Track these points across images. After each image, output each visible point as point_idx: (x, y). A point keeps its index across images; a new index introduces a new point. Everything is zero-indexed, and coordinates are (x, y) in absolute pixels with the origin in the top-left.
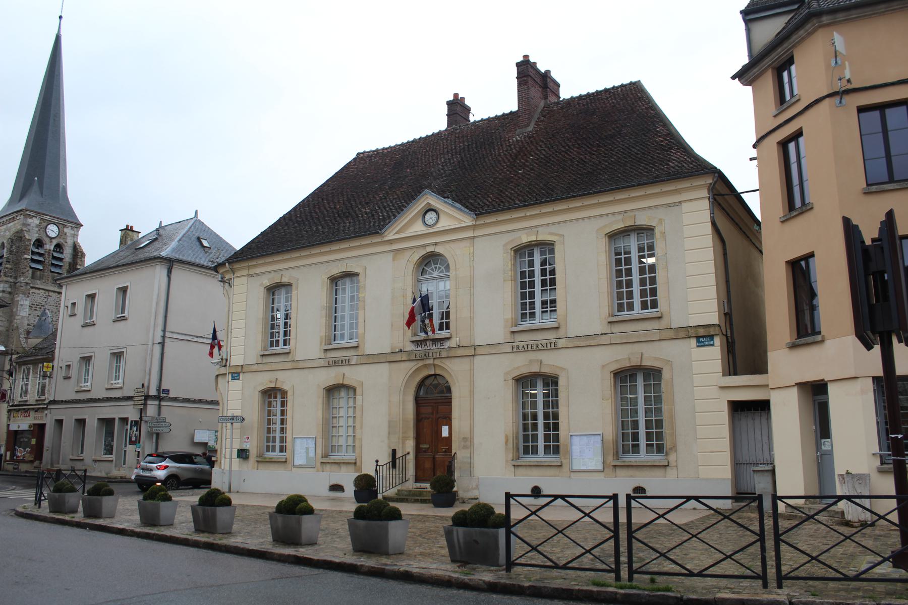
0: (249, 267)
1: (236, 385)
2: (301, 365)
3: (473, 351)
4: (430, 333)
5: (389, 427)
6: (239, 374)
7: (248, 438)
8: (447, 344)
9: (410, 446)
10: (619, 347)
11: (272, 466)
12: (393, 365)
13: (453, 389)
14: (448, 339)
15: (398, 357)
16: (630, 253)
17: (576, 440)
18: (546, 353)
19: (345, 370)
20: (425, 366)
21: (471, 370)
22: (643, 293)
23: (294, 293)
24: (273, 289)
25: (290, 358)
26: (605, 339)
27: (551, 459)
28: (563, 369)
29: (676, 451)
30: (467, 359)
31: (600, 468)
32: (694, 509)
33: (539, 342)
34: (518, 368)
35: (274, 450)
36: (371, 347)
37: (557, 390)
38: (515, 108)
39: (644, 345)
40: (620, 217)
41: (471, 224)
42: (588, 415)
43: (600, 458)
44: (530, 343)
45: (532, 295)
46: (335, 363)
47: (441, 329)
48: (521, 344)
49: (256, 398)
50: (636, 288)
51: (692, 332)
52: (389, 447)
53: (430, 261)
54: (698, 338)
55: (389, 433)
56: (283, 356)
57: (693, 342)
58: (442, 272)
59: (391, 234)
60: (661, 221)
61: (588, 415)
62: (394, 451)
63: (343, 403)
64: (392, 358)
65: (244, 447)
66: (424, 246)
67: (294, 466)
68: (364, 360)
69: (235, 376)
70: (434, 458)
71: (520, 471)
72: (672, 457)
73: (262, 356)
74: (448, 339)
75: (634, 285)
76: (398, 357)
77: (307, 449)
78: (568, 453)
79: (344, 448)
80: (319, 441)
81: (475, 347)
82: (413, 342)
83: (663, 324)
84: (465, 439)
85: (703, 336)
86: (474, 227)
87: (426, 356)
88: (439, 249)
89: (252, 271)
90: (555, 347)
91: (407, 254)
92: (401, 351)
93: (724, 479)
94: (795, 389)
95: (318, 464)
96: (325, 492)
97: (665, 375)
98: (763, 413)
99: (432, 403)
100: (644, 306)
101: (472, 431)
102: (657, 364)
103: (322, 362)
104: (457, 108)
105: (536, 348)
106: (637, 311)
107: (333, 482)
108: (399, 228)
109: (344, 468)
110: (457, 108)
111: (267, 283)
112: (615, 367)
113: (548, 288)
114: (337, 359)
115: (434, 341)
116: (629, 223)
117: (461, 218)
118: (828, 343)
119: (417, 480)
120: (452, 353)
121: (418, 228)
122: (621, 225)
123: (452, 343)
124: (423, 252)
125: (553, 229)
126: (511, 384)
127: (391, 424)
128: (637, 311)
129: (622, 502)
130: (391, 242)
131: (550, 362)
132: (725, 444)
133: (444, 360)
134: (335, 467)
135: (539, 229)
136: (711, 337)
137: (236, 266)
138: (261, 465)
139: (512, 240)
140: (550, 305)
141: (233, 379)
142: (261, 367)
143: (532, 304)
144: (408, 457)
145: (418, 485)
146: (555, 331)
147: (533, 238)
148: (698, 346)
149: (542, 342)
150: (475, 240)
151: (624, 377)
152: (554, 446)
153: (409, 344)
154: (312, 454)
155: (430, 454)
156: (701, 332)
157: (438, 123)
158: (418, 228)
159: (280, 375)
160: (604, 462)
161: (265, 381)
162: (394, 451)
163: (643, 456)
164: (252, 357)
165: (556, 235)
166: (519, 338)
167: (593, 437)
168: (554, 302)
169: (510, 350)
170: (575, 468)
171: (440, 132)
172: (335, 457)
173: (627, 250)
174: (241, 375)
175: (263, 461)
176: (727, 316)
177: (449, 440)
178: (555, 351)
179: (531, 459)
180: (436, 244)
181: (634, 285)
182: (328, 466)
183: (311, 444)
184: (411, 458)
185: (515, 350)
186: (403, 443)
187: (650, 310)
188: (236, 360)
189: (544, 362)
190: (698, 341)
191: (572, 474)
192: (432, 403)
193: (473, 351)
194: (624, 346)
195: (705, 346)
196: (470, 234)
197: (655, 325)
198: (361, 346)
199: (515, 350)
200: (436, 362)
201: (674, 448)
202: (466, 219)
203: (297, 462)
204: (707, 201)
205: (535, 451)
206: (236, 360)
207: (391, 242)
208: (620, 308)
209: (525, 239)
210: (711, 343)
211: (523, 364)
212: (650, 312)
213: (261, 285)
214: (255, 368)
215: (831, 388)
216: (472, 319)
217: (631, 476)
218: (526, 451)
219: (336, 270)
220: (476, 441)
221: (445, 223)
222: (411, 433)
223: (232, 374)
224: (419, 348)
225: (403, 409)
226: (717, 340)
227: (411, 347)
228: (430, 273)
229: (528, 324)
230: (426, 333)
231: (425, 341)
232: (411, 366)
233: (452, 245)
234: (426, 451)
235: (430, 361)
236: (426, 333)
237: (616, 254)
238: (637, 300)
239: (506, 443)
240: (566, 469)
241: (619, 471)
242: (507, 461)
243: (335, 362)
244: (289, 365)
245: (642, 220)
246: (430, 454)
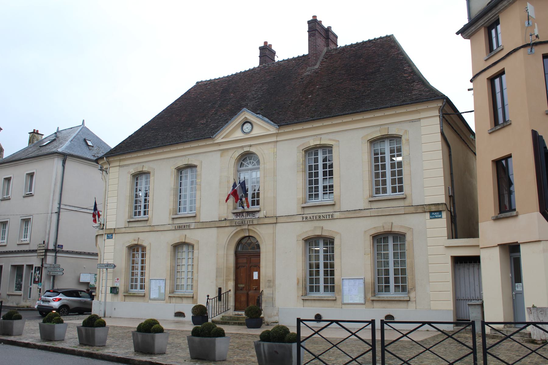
0: (120, 160)
1: (110, 242)
3: (276, 220)
4: (246, 207)
5: (217, 272)
6: (112, 234)
7: (118, 279)
8: (257, 215)
9: (231, 285)
10: (377, 218)
11: (134, 298)
13: (261, 246)
14: (258, 211)
15: (223, 224)
16: (384, 153)
17: (346, 282)
18: (326, 222)
20: (242, 230)
21: (274, 234)
22: (393, 181)
23: (152, 178)
24: (137, 176)
25: (148, 224)
26: (367, 213)
27: (329, 295)
28: (337, 233)
29: (415, 290)
30: (272, 226)
31: (362, 301)
32: (428, 331)
33: (321, 215)
34: (306, 232)
35: (136, 288)
36: (204, 217)
37: (333, 248)
38: (306, 52)
39: (394, 217)
40: (378, 128)
41: (275, 132)
42: (354, 264)
43: (362, 295)
44: (315, 215)
45: (317, 182)
46: (180, 228)
47: (253, 204)
48: (308, 216)
49: (124, 251)
50: (389, 178)
51: (427, 208)
52: (217, 286)
53: (246, 158)
54: (431, 212)
55: (217, 277)
56: (143, 222)
57: (428, 215)
58: (255, 165)
59: (219, 138)
60: (406, 132)
61: (354, 264)
62: (220, 289)
63: (185, 255)
64: (219, 224)
65: (115, 286)
67: (150, 299)
68: (199, 225)
70: (248, 294)
71: (307, 303)
72: (412, 295)
73: (129, 222)
74: (258, 211)
75: (387, 176)
76: (223, 224)
77: (159, 287)
78: (341, 291)
79: (185, 286)
80: (168, 282)
81: (277, 218)
82: (234, 213)
83: (407, 203)
84: (269, 281)
85: (434, 211)
86: (277, 135)
87: (242, 223)
88: (252, 150)
89: (122, 163)
90: (332, 218)
91: (230, 153)
92: (225, 220)
93: (448, 310)
94: (498, 249)
95: (167, 298)
96: (172, 317)
97: (408, 238)
98: (476, 266)
99: (247, 255)
100: (394, 190)
101: (274, 275)
102: (402, 230)
103: (171, 227)
104: (266, 52)
105: (319, 218)
106: (389, 193)
107: (177, 310)
108: (225, 134)
109: (185, 300)
110: (266, 52)
111: (132, 170)
112: (373, 232)
113: (328, 177)
114: (181, 225)
115: (248, 213)
116: (384, 133)
117: (268, 128)
118: (520, 217)
119: (236, 309)
120: (261, 221)
121: (239, 134)
122: (378, 134)
123: (261, 215)
124: (241, 151)
125: (331, 136)
126: (301, 244)
127: (218, 270)
128: (389, 193)
129: (378, 325)
130: (219, 144)
131: (328, 228)
132: (449, 286)
133: (254, 226)
134: (179, 300)
135: (322, 136)
136: (440, 212)
137: (111, 159)
138: (126, 298)
139: (303, 144)
140: (328, 189)
141: (108, 238)
142: (128, 230)
143: (317, 188)
144: (230, 293)
145: (237, 313)
146: (331, 207)
147: (318, 142)
148: (431, 218)
149: (323, 214)
150: (278, 143)
151: (380, 239)
152: (330, 287)
153: (232, 215)
154: (162, 291)
155: (244, 292)
156: (433, 208)
157: (254, 62)
158: (239, 134)
159: (141, 236)
160: (365, 298)
161: (130, 239)
162: (220, 289)
163: (392, 294)
164: (122, 224)
165: (334, 140)
166: (307, 211)
167: (358, 280)
168: (331, 187)
169: (301, 220)
170: (345, 302)
171: (254, 69)
172: (179, 293)
173: (383, 151)
174: (114, 235)
175: (128, 295)
176: (451, 198)
177: (258, 282)
178: (332, 221)
179: (315, 295)
180: (250, 146)
181: (387, 176)
183: (162, 284)
184: (232, 294)
185: (304, 220)
186: (227, 284)
187: (398, 193)
188: (110, 225)
189: (325, 228)
190: (431, 215)
191: (343, 306)
192: (247, 255)
193: (276, 220)
194: (380, 217)
195: (435, 218)
196: (274, 139)
197: (401, 203)
198: (198, 216)
199: (304, 220)
200: (250, 227)
201: (414, 288)
202: (272, 129)
203: (152, 297)
204: (438, 118)
205: (318, 289)
206: (110, 225)
207: (219, 144)
208: (377, 191)
209: (312, 143)
210: (440, 216)
211: (310, 229)
212: (398, 194)
213: (129, 172)
214: (124, 230)
215: (522, 248)
216: (275, 198)
217: (384, 308)
218: (311, 289)
219: (181, 163)
220: (277, 282)
221: (256, 132)
222: (232, 277)
223: (108, 234)
224: (238, 218)
225: (227, 260)
226: (444, 214)
228: (246, 166)
229: (313, 202)
230: (243, 207)
231: (242, 213)
232: (233, 230)
233: (262, 147)
234: (242, 289)
235: (246, 227)
236: (243, 207)
237: (375, 154)
238: (389, 186)
239: (298, 284)
240: (339, 302)
241: (376, 304)
242: (298, 296)
243: (180, 227)
244: (147, 229)
245: (393, 131)
246: (244, 292)
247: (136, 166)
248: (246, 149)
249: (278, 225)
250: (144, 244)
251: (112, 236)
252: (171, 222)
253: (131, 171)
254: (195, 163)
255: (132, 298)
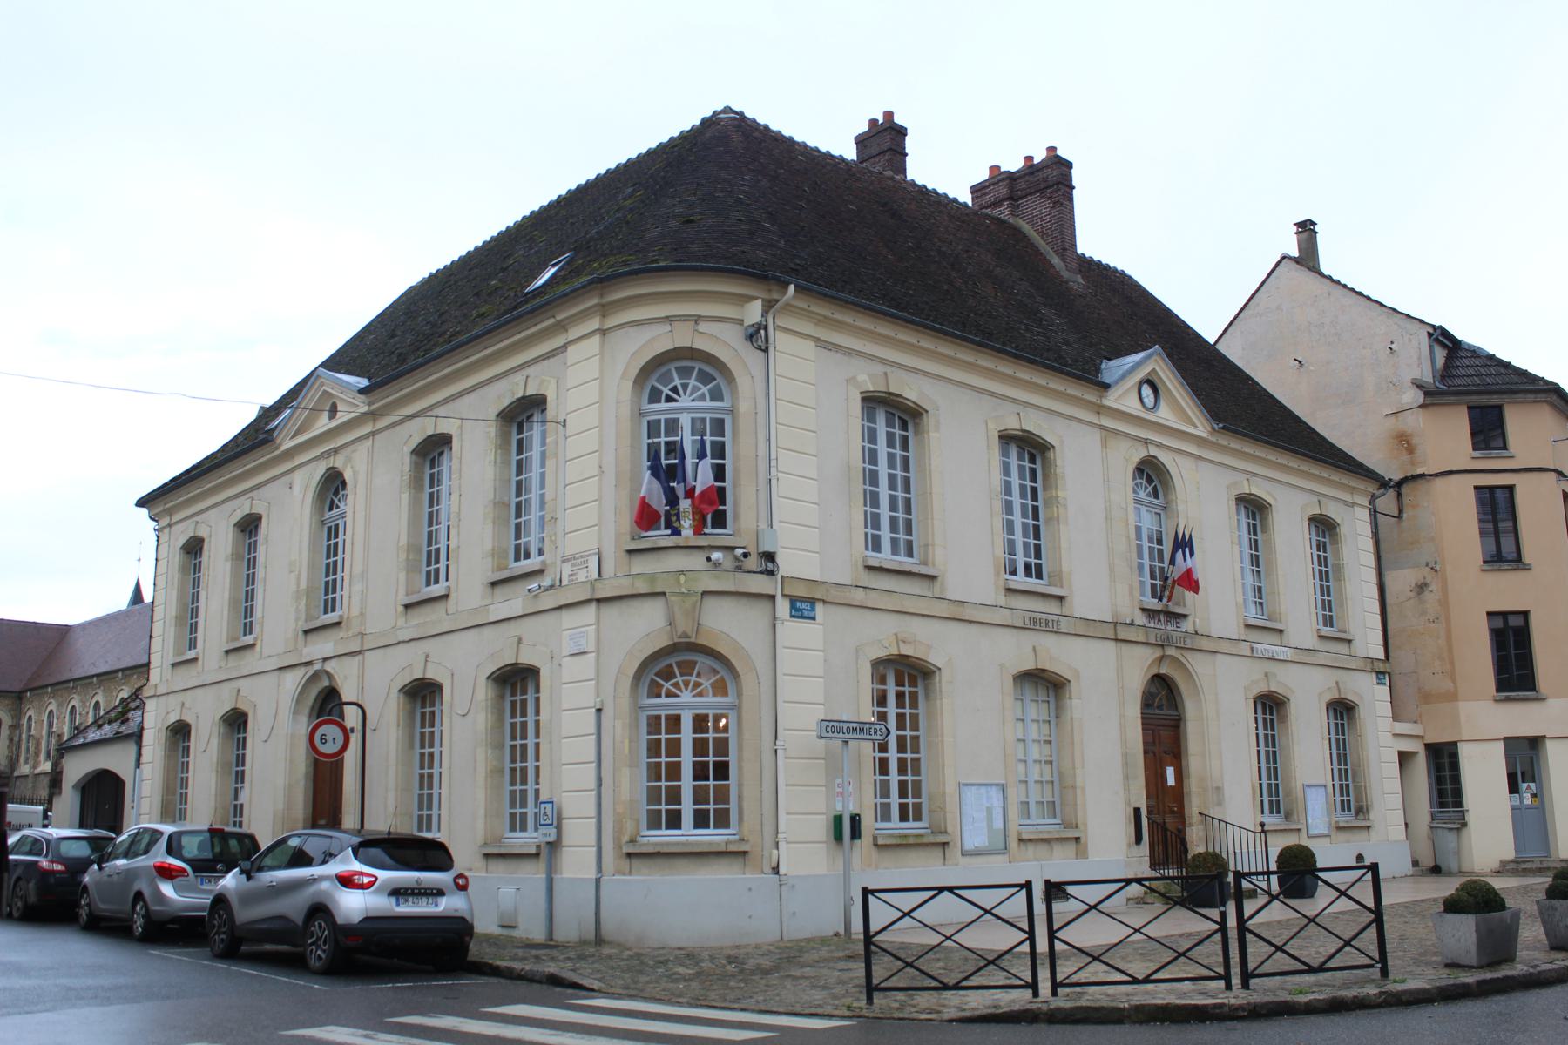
1: (792, 631)
2: (968, 613)
6: (812, 601)
12: (1125, 647)
19: (1048, 642)
40: (1315, 499)
41: (1204, 435)
46: (1036, 625)
52: (1128, 802)
54: (1378, 673)
64: (1115, 632)
66: (1146, 442)
69: (803, 607)
74: (1185, 616)
77: (989, 810)
82: (1143, 610)
92: (1131, 624)
94: (1501, 744)
95: (1013, 844)
104: (886, 139)
114: (1038, 616)
118: (1550, 701)
123: (1187, 626)
134: (1042, 848)
141: (797, 613)
150: (1202, 463)
153: (1138, 613)
157: (837, 139)
161: (882, 636)
174: (819, 608)
180: (1159, 445)
182: (1031, 848)
203: (969, 845)
207: (1100, 409)
213: (851, 381)
215: (1549, 744)
219: (1012, 424)
220: (1227, 792)
221: (1164, 414)
227: (1141, 619)
231: (1159, 612)
232: (1150, 654)
247: (879, 369)
248: (1154, 451)
249: (1219, 656)
250: (935, 659)
251: (813, 609)
252: (1002, 599)
253: (862, 377)
254: (1049, 438)
255: (902, 853)
